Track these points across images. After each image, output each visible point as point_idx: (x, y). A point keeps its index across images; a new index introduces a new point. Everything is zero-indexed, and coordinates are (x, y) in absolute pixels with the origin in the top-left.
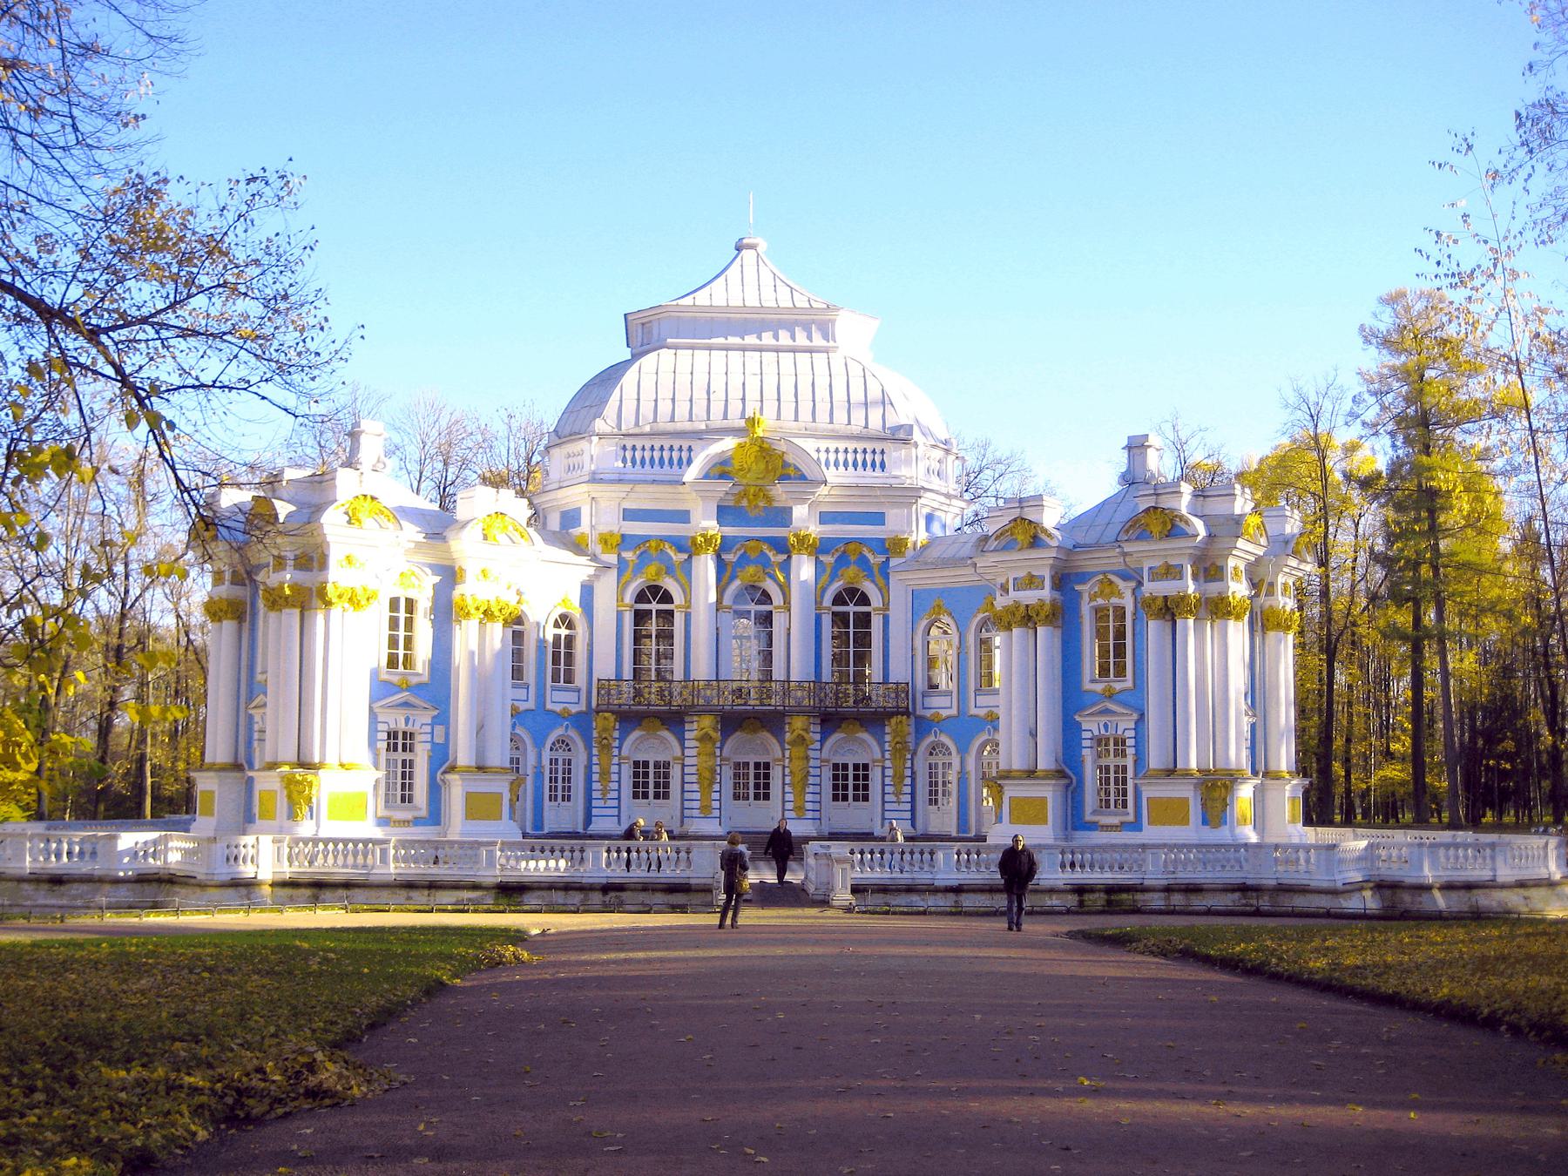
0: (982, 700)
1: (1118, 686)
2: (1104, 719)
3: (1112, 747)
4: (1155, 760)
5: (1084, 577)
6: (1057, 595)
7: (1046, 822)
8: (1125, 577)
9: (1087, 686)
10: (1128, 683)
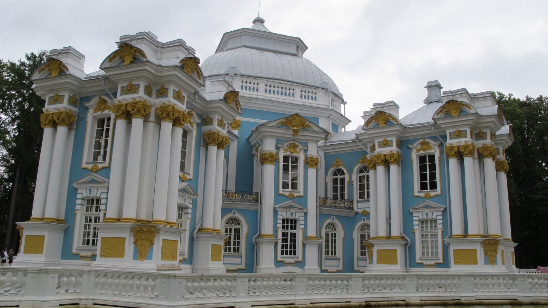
0: (361, 205)
1: (432, 194)
2: (426, 211)
3: (429, 225)
4: (457, 229)
5: (413, 141)
6: (399, 150)
7: (396, 262)
8: (435, 138)
9: (416, 194)
10: (438, 191)
